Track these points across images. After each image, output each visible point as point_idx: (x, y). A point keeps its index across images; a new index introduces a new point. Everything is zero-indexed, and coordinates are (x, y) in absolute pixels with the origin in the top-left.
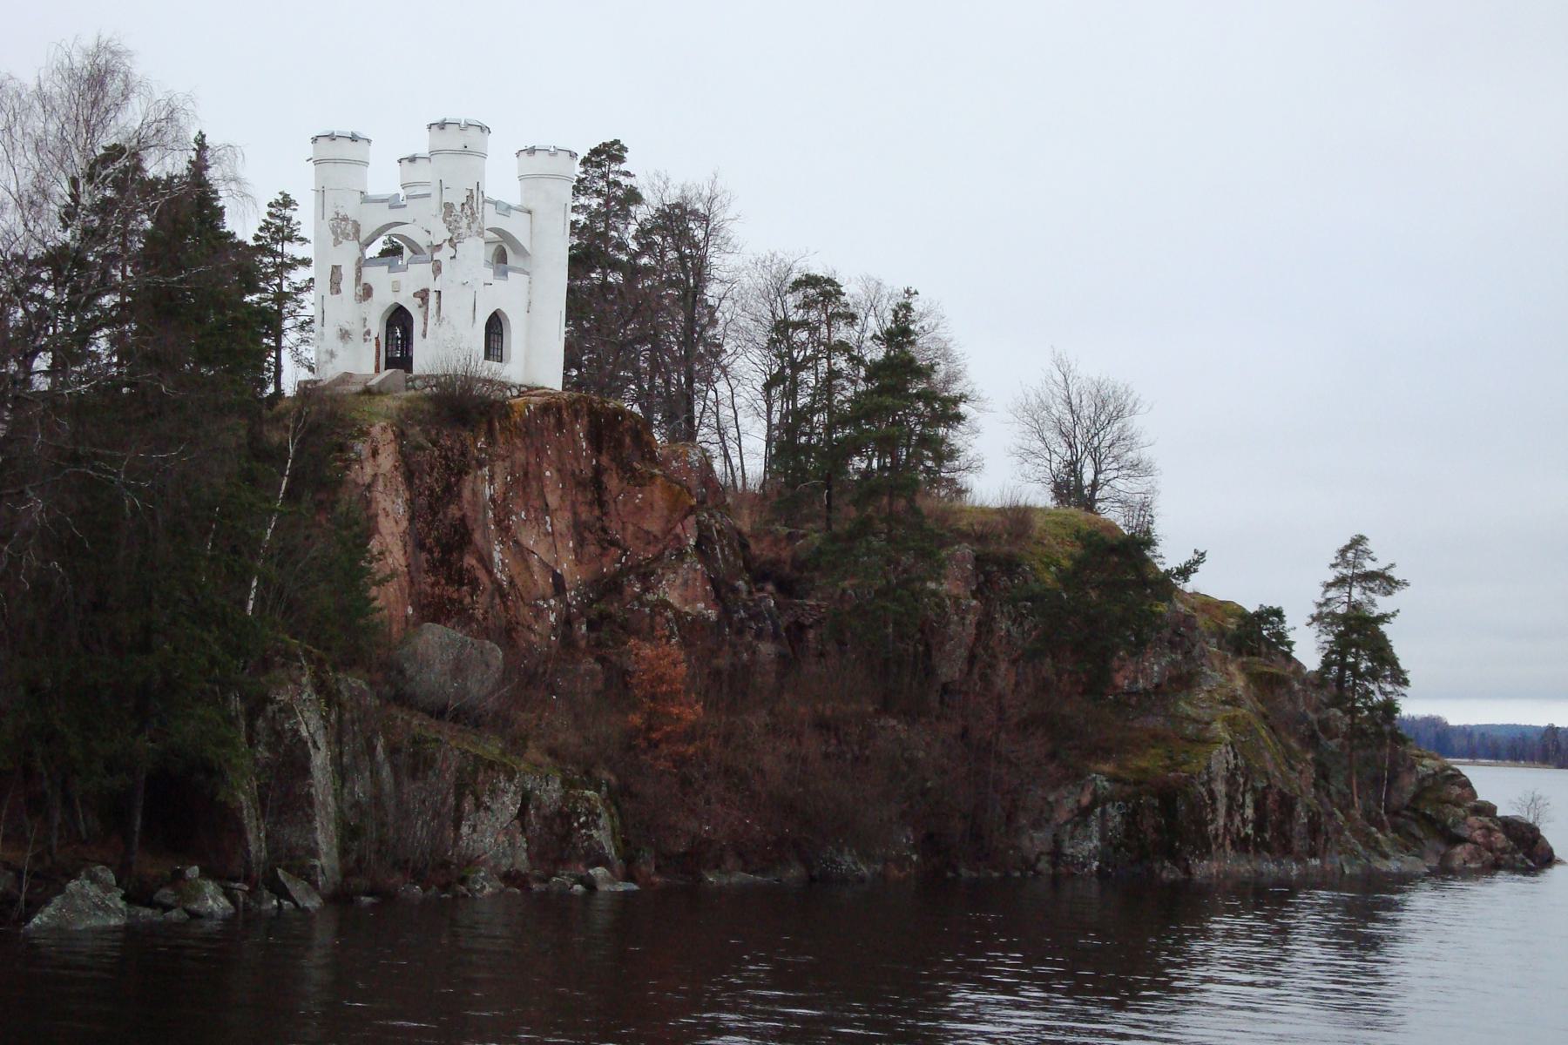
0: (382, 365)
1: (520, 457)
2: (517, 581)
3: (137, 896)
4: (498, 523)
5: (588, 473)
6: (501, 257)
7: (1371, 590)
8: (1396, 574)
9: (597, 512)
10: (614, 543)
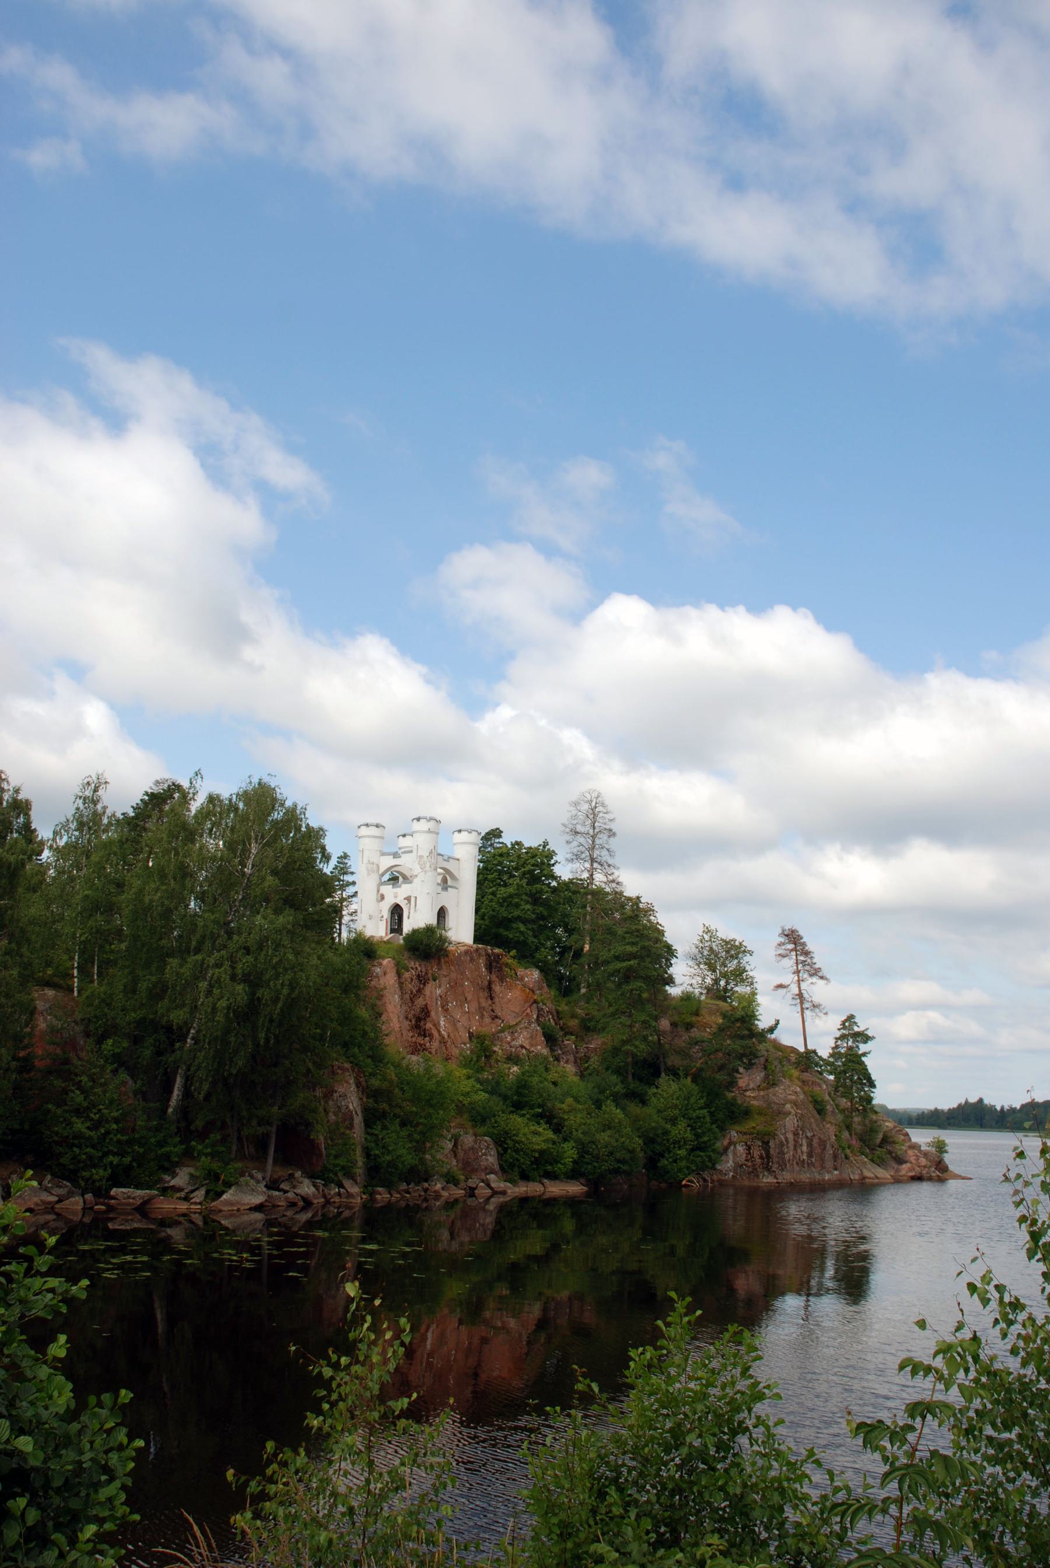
0: (389, 932)
1: (453, 975)
2: (452, 1035)
3: (273, 1185)
4: (442, 1008)
6: (445, 880)
7: (857, 1041)
8: (870, 1033)
9: (490, 1002)
10: (496, 1017)
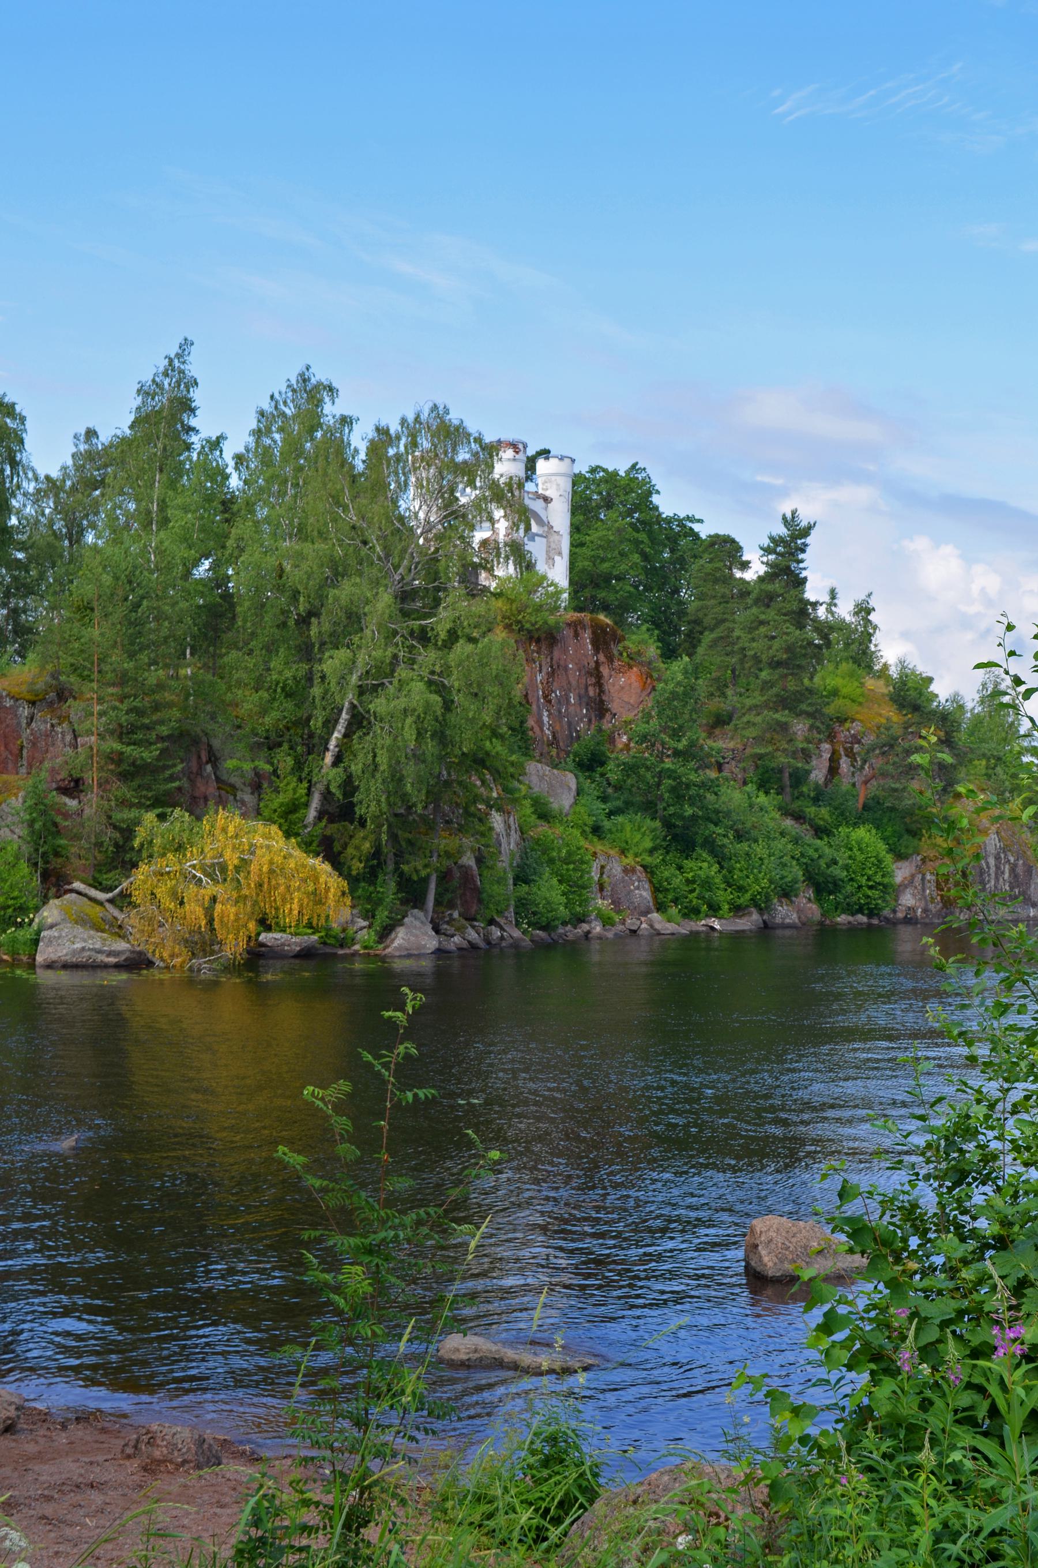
5: (592, 665)
